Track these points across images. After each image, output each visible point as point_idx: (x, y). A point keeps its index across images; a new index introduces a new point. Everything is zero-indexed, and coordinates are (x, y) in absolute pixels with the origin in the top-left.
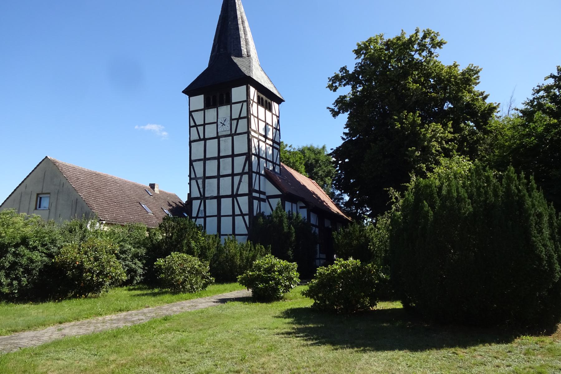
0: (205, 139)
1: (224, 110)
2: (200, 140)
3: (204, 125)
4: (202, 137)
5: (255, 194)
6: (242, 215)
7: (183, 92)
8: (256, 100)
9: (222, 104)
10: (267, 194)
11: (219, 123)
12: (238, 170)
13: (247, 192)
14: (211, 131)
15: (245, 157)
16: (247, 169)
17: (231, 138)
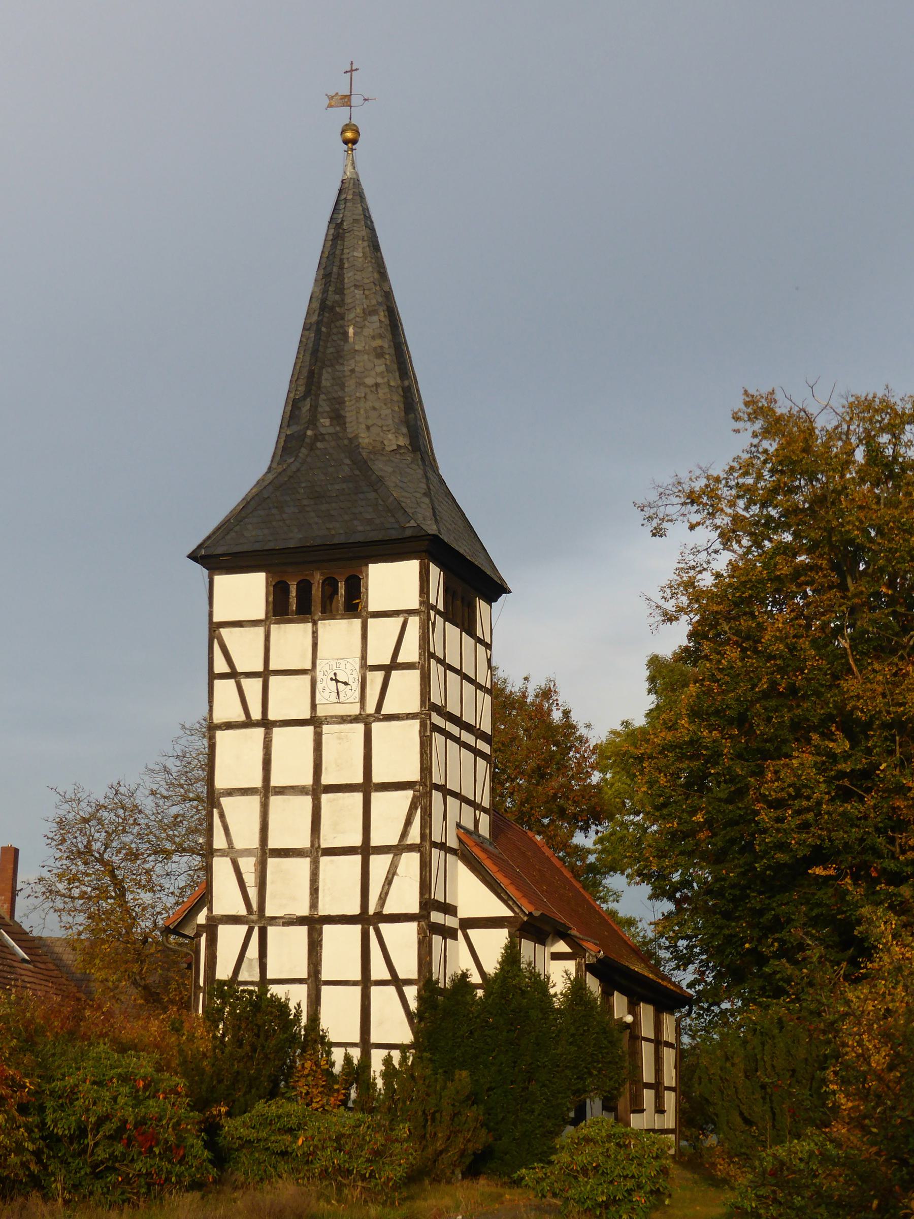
0: (267, 724)
1: (339, 634)
2: (248, 723)
3: (265, 674)
4: (256, 715)
5: (437, 917)
6: (397, 982)
7: (193, 556)
8: (441, 607)
9: (329, 613)
10: (463, 913)
11: (319, 675)
12: (385, 832)
13: (415, 909)
14: (288, 698)
15: (409, 794)
16: (414, 836)
17: (360, 727)
